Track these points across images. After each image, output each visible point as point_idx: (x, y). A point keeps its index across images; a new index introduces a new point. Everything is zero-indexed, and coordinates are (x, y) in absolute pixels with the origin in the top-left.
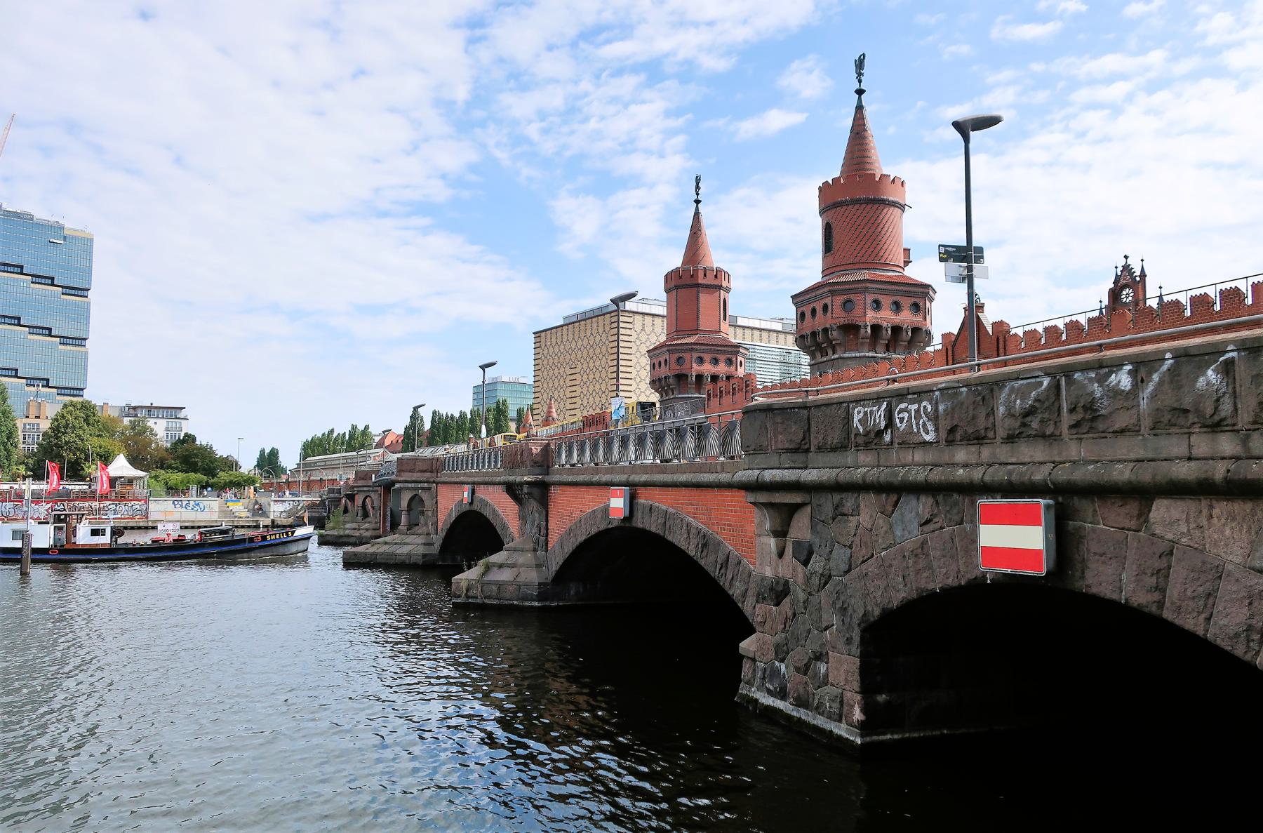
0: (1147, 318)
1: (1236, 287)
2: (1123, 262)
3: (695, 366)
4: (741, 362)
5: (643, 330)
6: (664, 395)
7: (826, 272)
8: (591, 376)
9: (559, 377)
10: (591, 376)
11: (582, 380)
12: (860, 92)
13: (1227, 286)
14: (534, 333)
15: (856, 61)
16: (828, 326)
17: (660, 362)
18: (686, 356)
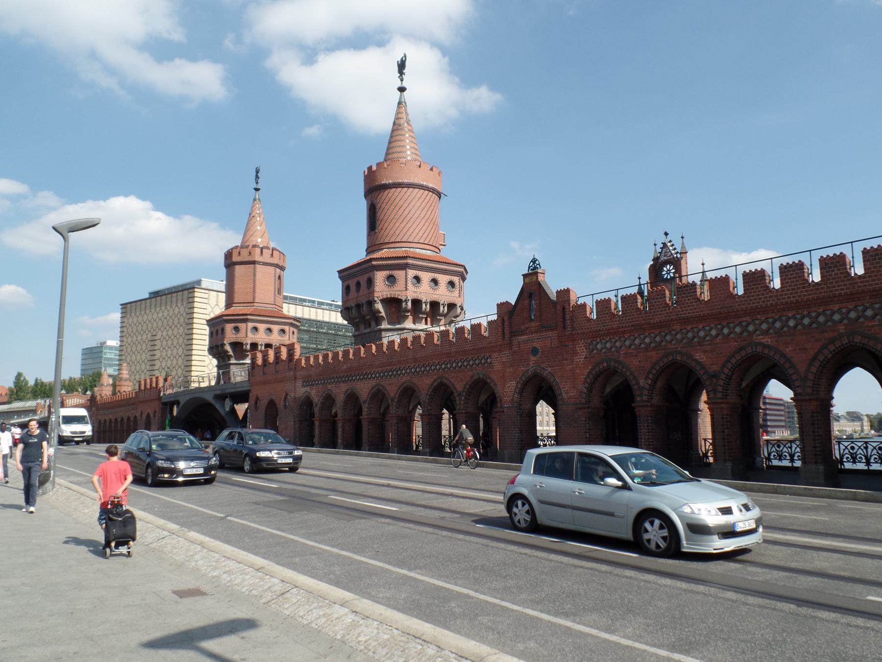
0: (759, 284)
1: (800, 261)
2: (663, 239)
3: (250, 334)
4: (293, 333)
5: (217, 305)
6: (221, 361)
7: (370, 249)
8: (170, 342)
9: (142, 342)
10: (170, 342)
11: (162, 345)
12: (402, 90)
13: (831, 252)
14: (121, 305)
15: (398, 62)
16: (371, 299)
17: (217, 331)
18: (242, 326)
